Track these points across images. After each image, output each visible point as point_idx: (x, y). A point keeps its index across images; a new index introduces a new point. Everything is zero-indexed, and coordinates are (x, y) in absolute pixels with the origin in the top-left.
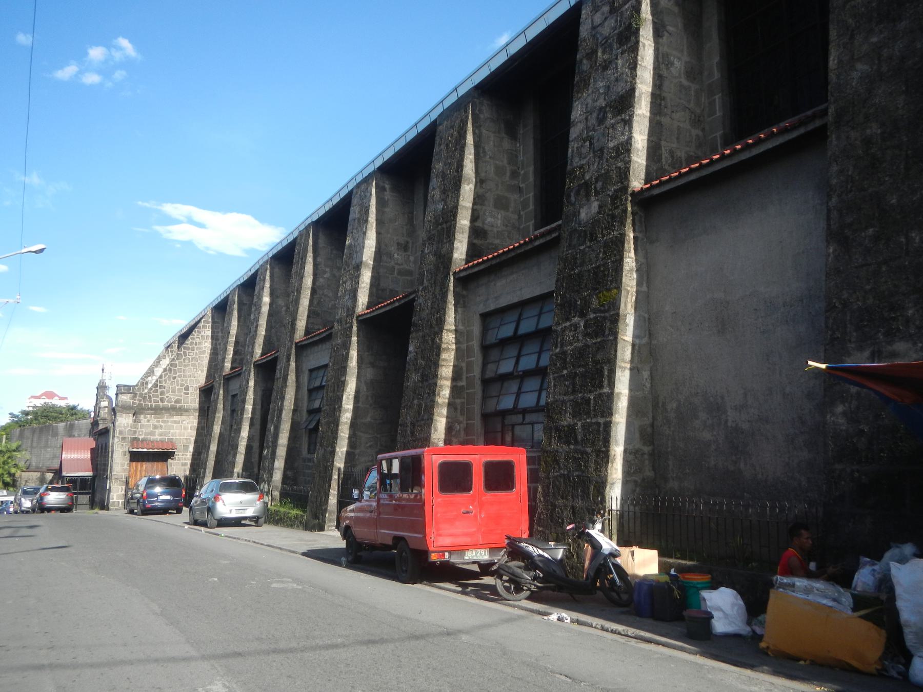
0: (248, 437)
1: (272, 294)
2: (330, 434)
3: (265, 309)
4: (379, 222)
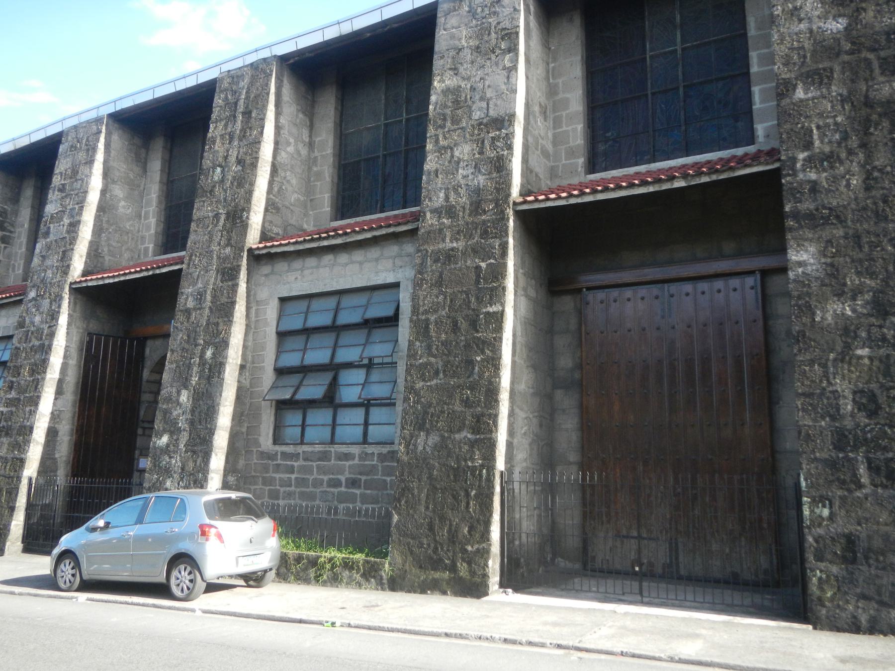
0: (52, 413)
1: (106, 175)
2: (458, 407)
3: (93, 198)
4: (528, 61)
